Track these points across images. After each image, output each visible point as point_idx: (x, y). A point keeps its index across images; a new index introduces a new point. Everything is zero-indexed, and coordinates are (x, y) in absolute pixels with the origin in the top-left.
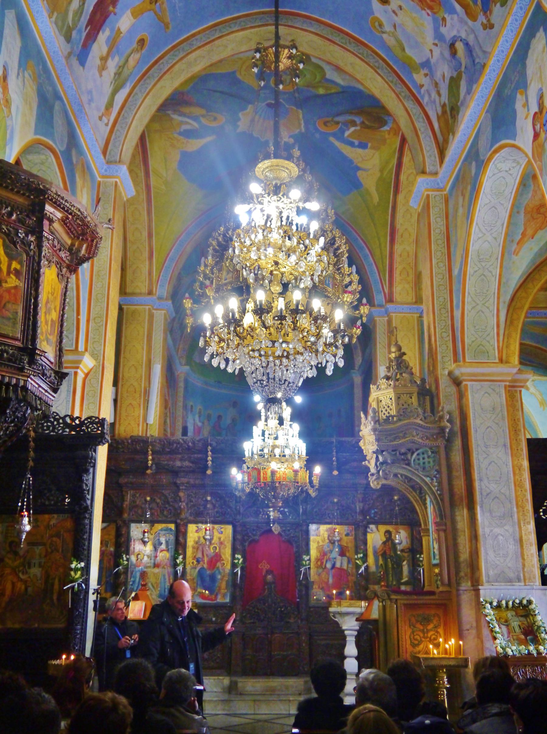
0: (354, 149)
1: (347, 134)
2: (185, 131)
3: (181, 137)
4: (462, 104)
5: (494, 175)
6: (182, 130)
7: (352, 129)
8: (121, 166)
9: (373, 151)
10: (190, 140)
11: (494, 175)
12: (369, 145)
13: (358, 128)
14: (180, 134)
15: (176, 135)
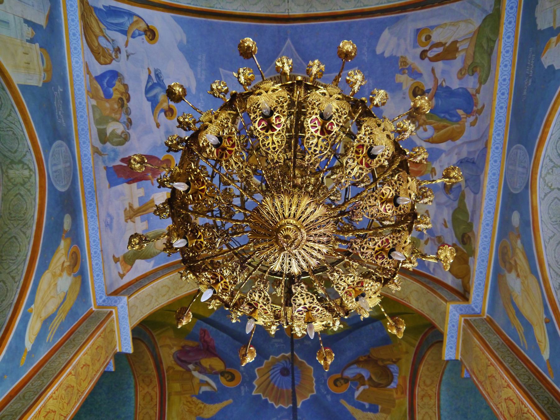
0: (365, 413)
1: (357, 394)
2: (205, 393)
3: (200, 401)
4: (474, 212)
5: (546, 195)
6: (201, 392)
7: (361, 388)
8: (122, 297)
9: (385, 415)
10: (208, 405)
11: (546, 195)
12: (380, 407)
13: (367, 387)
14: (199, 397)
15: (194, 399)
